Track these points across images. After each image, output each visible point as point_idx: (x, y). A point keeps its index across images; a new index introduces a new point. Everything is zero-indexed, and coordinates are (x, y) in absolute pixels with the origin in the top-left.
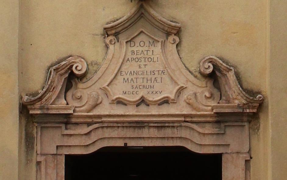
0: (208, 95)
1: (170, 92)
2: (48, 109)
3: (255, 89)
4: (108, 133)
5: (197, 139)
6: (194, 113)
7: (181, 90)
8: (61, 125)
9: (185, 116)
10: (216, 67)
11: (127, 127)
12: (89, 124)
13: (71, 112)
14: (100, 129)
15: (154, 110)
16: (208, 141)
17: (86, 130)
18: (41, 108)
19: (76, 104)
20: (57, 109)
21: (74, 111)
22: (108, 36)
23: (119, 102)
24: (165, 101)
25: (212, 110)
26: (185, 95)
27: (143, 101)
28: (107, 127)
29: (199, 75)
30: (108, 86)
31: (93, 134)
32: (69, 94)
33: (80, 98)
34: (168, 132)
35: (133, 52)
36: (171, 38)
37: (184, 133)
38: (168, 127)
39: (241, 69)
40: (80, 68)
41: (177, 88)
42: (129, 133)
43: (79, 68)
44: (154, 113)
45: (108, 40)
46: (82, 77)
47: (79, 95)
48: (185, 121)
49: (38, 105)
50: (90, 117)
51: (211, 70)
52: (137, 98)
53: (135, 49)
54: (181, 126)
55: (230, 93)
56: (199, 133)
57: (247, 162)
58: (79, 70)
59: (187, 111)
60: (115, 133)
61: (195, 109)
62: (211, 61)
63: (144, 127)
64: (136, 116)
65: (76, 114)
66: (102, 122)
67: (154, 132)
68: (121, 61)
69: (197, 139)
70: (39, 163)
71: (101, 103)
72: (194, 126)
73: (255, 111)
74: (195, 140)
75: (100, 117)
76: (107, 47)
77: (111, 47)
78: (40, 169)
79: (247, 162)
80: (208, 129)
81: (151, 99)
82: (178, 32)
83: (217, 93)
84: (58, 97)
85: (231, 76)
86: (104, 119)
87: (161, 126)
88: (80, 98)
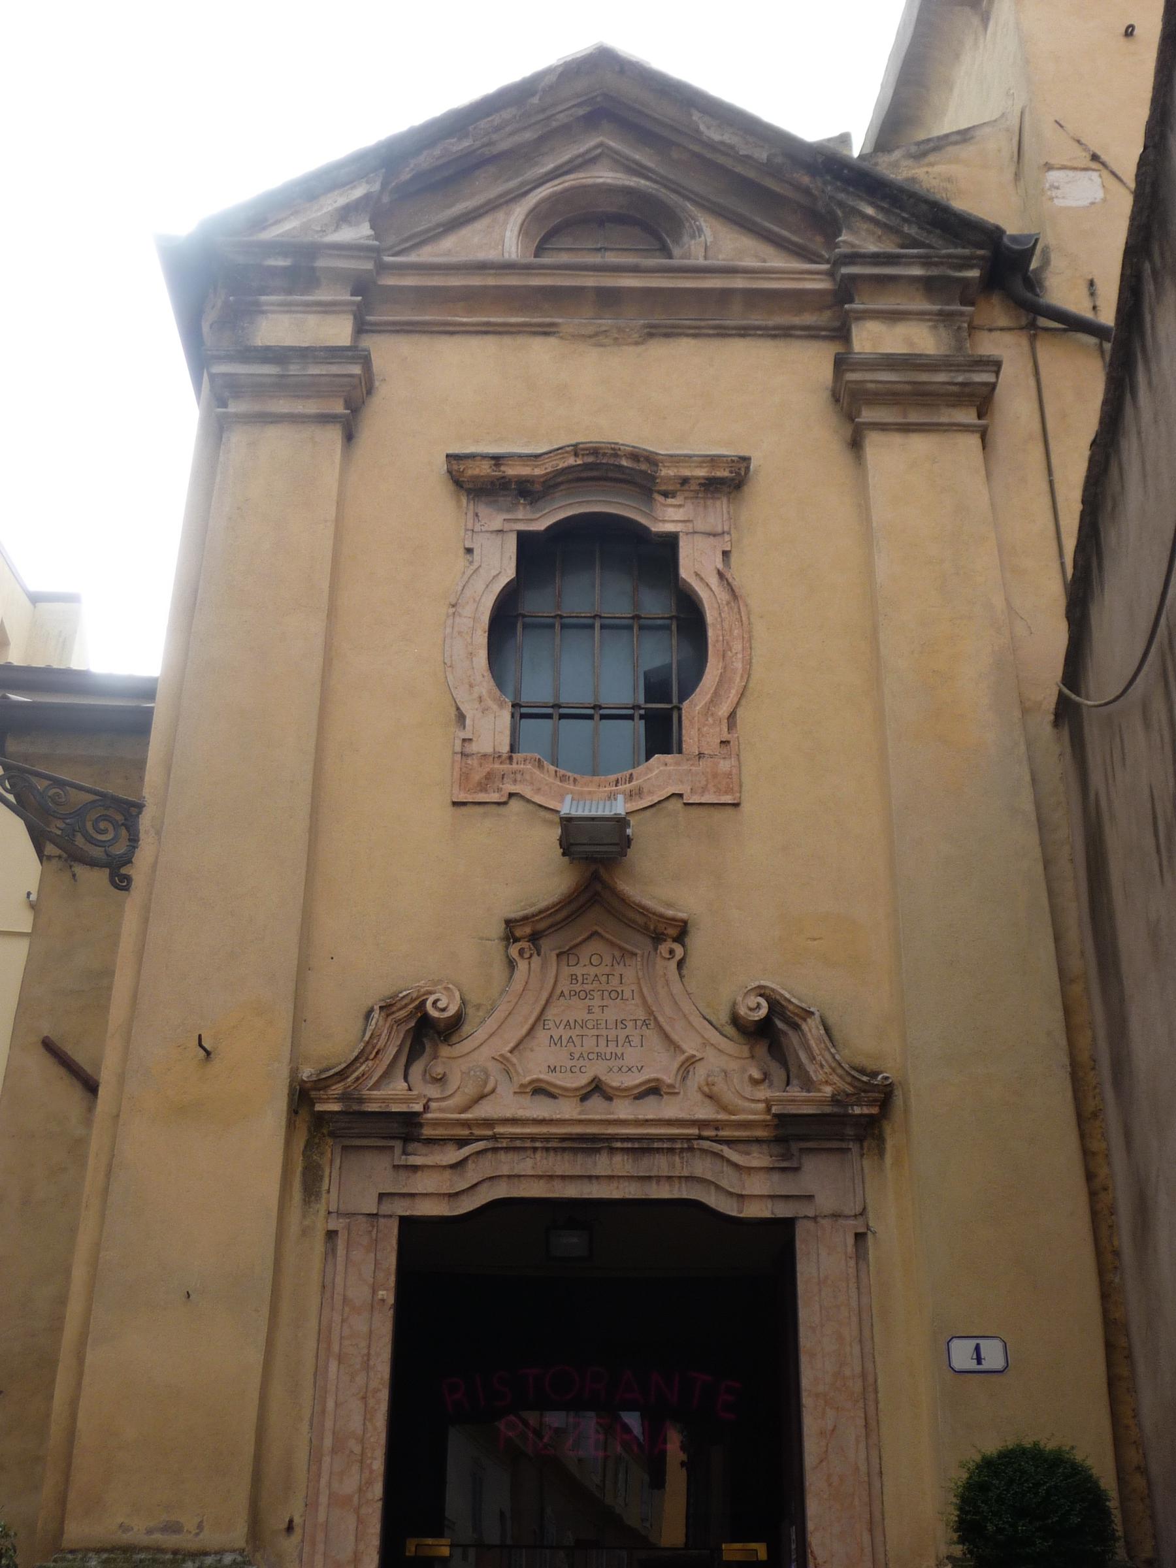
0: (757, 1075)
1: (662, 1067)
2: (361, 1101)
3: (871, 1065)
4: (507, 1164)
5: (729, 1180)
6: (722, 1116)
7: (689, 1064)
8: (391, 1143)
9: (702, 1124)
10: (776, 1006)
11: (555, 1149)
12: (462, 1142)
13: (418, 1107)
14: (489, 1155)
15: (623, 1110)
16: (757, 1185)
17: (452, 1155)
18: (344, 1098)
19: (432, 1091)
20: (384, 1100)
21: (426, 1108)
22: (516, 940)
23: (540, 1090)
24: (653, 1090)
25: (768, 1109)
26: (699, 1075)
27: (596, 1088)
28: (507, 1149)
29: (730, 1030)
30: (511, 1052)
31: (470, 1165)
32: (417, 1069)
33: (440, 1080)
34: (661, 1165)
35: (573, 978)
36: (664, 948)
37: (701, 1167)
38: (658, 1150)
39: (831, 1020)
40: (444, 1005)
41: (682, 1058)
42: (563, 1165)
43: (440, 1005)
44: (622, 1116)
45: (514, 951)
46: (450, 1029)
47: (439, 1070)
48: (700, 1138)
49: (337, 1089)
50: (466, 1124)
51: (763, 1012)
52: (583, 1080)
53: (578, 971)
54: (691, 1149)
55: (811, 1069)
56: (736, 1166)
57: (860, 1237)
58: (443, 1010)
59: (705, 1112)
60: (525, 1165)
61: (725, 1108)
62: (762, 991)
63: (598, 1150)
64: (580, 1121)
65: (429, 1116)
66: (494, 1137)
67: (621, 1164)
68: (545, 995)
69: (729, 1180)
70: (331, 1235)
71: (493, 1091)
72: (727, 1151)
73: (874, 1110)
74: (724, 1183)
75: (488, 1123)
76: (511, 965)
77: (522, 965)
78: (334, 1251)
79: (860, 1237)
80: (757, 1158)
81: (615, 1084)
82: (681, 931)
83: (778, 1073)
84: (387, 1074)
85: (812, 1029)
86: (500, 1130)
87: (642, 1147)
88: (440, 1080)
